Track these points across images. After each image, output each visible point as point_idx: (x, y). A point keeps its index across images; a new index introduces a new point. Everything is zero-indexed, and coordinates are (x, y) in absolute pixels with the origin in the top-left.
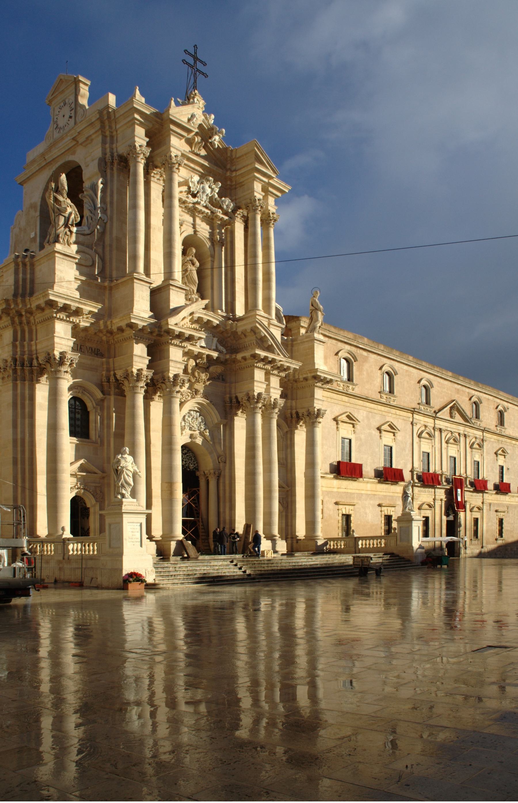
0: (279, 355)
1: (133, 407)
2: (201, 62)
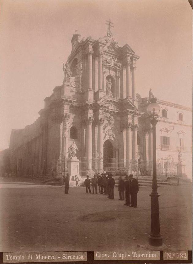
2: (112, 23)
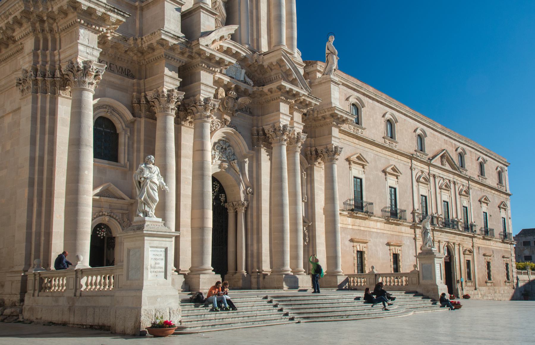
0: (302, 89)
1: (165, 129)
